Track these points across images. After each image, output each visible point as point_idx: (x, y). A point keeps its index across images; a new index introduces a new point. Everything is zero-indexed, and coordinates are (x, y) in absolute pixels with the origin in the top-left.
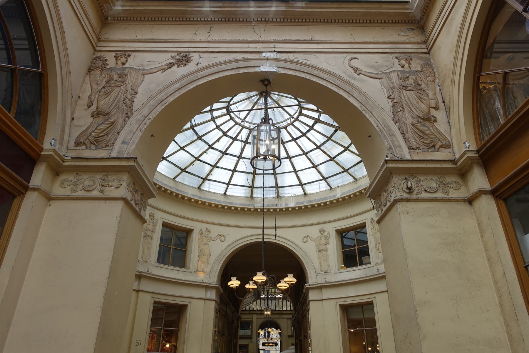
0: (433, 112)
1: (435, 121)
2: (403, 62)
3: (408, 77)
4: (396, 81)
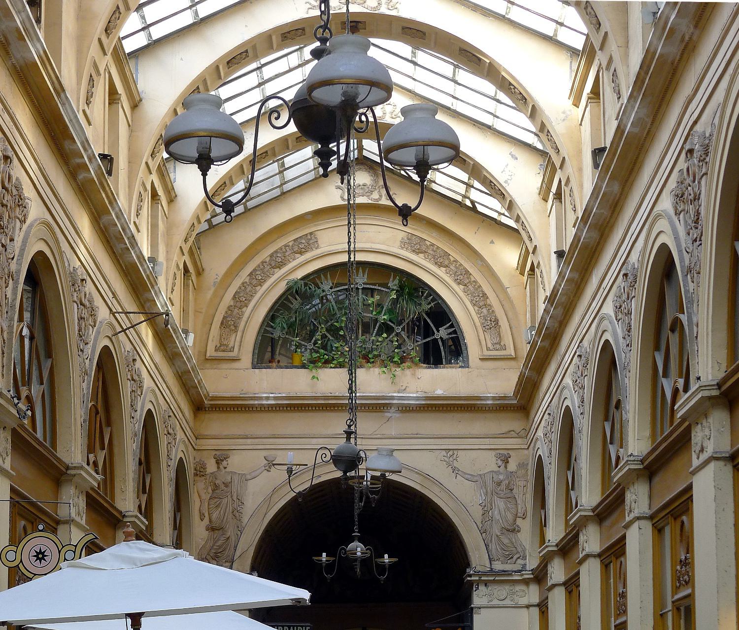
0: (519, 521)
1: (519, 531)
2: (500, 463)
3: (501, 482)
4: (490, 485)
